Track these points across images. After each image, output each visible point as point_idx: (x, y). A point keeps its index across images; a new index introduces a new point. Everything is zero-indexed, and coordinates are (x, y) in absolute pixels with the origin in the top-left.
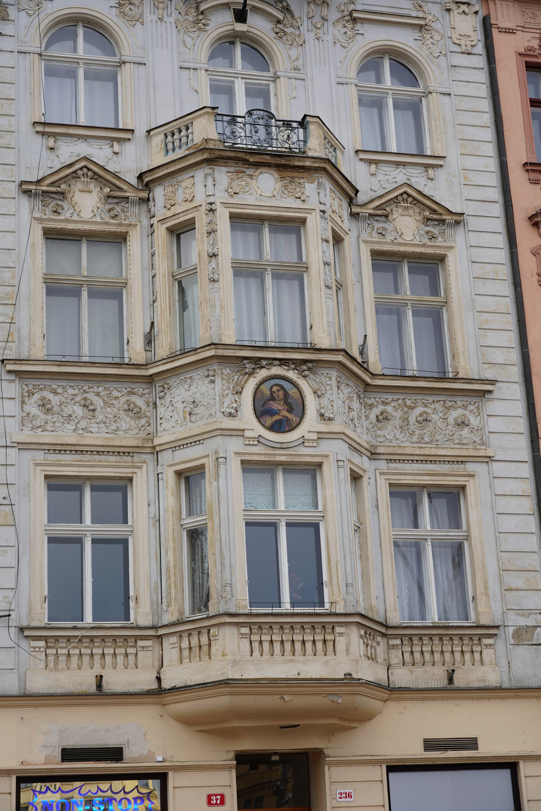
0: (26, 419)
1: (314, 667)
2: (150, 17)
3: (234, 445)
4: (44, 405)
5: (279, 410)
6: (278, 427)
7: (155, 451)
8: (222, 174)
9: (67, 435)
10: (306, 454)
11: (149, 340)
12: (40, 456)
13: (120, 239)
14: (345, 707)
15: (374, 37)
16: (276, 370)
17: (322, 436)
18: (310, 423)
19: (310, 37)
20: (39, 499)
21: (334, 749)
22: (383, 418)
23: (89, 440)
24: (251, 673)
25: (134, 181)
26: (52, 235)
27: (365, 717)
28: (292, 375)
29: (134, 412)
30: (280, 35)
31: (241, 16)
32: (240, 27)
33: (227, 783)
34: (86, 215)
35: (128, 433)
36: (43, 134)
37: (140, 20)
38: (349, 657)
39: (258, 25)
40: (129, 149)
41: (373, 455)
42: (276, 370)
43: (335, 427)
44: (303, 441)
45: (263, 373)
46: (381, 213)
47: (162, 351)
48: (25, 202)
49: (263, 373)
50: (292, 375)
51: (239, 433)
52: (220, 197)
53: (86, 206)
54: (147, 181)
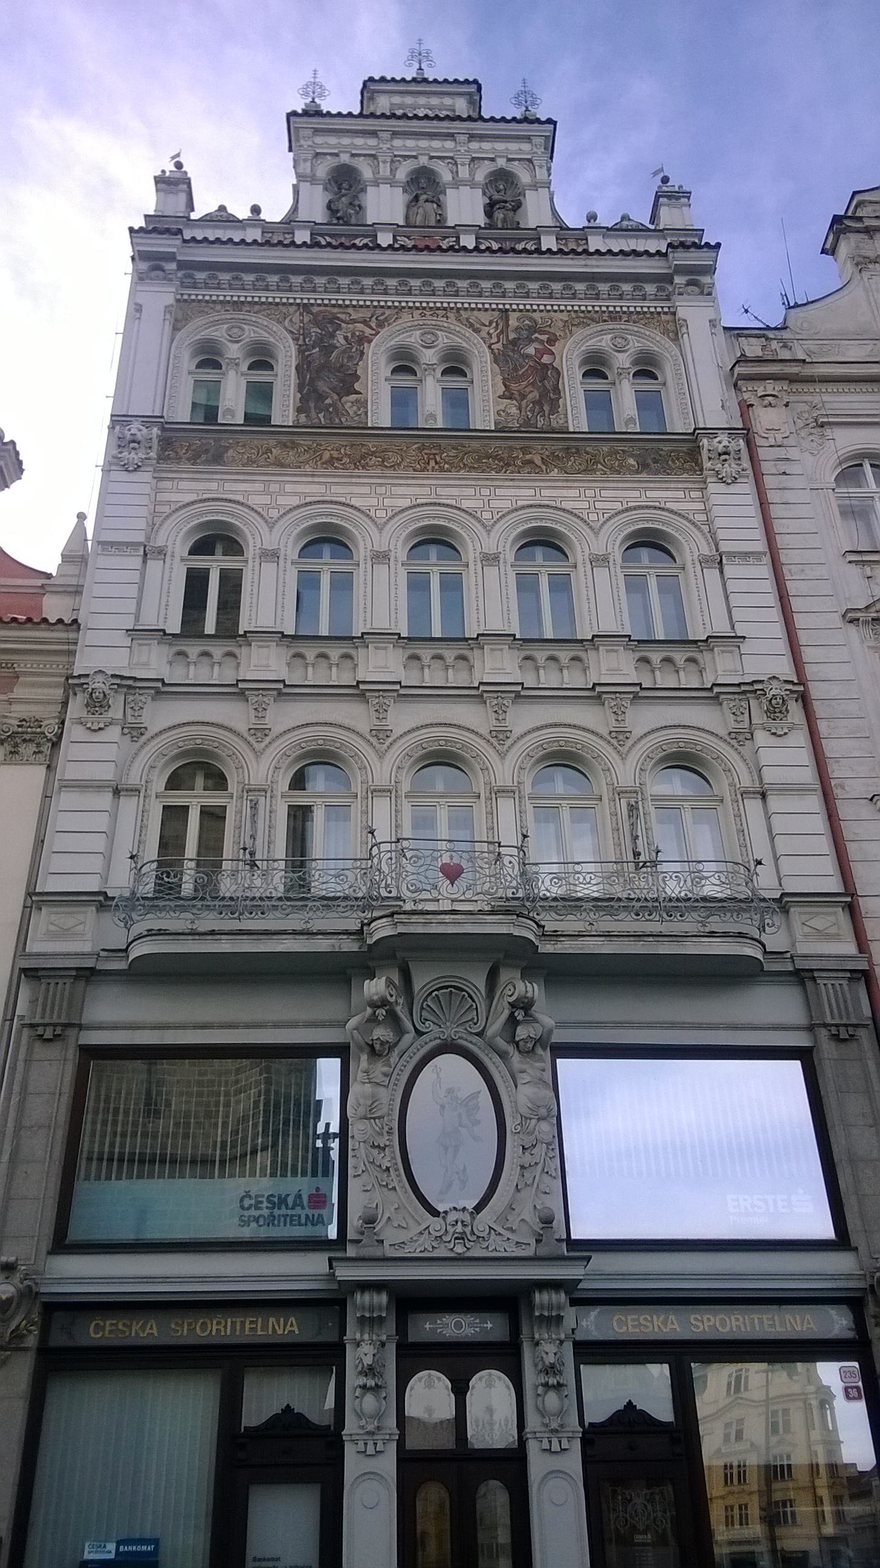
36: (857, 562)
48: (852, 630)
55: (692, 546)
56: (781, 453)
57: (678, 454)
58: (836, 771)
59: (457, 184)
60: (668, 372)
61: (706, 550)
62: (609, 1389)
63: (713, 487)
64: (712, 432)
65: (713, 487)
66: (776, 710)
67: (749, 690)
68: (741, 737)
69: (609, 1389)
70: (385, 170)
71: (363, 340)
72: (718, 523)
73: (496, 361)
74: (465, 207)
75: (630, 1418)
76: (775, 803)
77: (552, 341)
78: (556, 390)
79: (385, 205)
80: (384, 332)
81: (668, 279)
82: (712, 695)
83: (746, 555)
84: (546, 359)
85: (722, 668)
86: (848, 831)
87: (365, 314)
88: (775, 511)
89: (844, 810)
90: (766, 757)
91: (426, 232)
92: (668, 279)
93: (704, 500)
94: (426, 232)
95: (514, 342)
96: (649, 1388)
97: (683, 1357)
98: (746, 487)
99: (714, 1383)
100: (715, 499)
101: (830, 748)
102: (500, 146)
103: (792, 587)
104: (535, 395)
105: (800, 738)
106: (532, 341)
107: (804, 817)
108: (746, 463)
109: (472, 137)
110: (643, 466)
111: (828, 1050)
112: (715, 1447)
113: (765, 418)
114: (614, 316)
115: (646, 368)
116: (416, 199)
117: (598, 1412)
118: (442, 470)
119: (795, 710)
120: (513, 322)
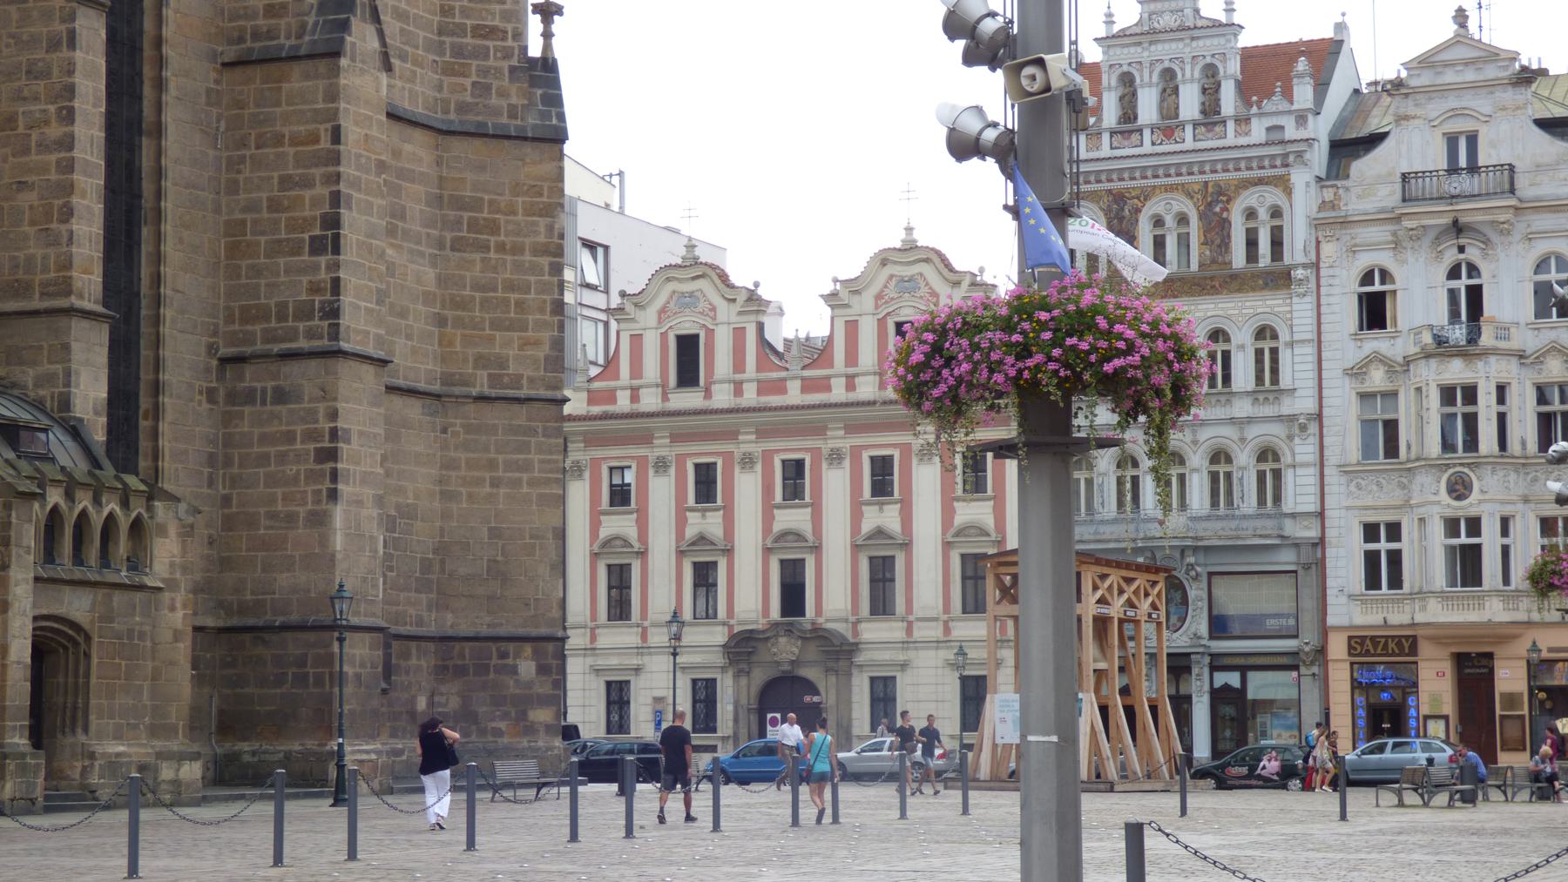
0: (1350, 494)
1: (1473, 616)
2: (1411, 260)
3: (1436, 509)
4: (1359, 487)
5: (1459, 489)
6: (1459, 498)
7: (1411, 507)
8: (1433, 362)
9: (1369, 502)
10: (1473, 512)
11: (1409, 447)
12: (1356, 512)
13: (1395, 394)
14: (1505, 634)
15: (1542, 247)
16: (1458, 469)
17: (1480, 502)
18: (1475, 495)
19: (1502, 256)
20: (1359, 533)
21: (1499, 652)
22: (1535, 480)
23: (1380, 503)
24: (1442, 619)
25: (1400, 360)
26: (1364, 396)
27: (1515, 637)
28: (1466, 470)
29: (1403, 487)
30: (1485, 256)
31: (1461, 249)
32: (1462, 256)
33: (1447, 667)
34: (1377, 382)
35: (1397, 497)
37: (1404, 262)
38: (1495, 611)
39: (1473, 254)
40: (1399, 341)
41: (1526, 500)
42: (1458, 469)
43: (1487, 497)
44: (1471, 505)
45: (1451, 471)
46: (1539, 359)
47: (1413, 456)
48: (1347, 380)
49: (1451, 471)
50: (1466, 470)
51: (1438, 503)
52: (1432, 376)
53: (1377, 379)
54: (1407, 362)
55: (1284, 336)
56: (1331, 272)
57: (1280, 279)
58: (1326, 453)
59: (1184, 82)
60: (1286, 215)
61: (1288, 339)
62: (1221, 679)
63: (1295, 300)
64: (1296, 267)
65: (1295, 300)
66: (1303, 428)
67: (1291, 418)
68: (1290, 438)
69: (1221, 679)
70: (1146, 78)
71: (1138, 211)
72: (1295, 322)
73: (1200, 218)
74: (1190, 103)
75: (1226, 687)
76: (1299, 471)
77: (1228, 201)
78: (1229, 236)
79: (1148, 109)
80: (1148, 204)
81: (1286, 155)
82: (1280, 418)
83: (1303, 341)
84: (1225, 215)
85: (1287, 407)
86: (1327, 480)
87: (1138, 192)
88: (1323, 309)
89: (1327, 471)
90: (1298, 449)
91: (1169, 126)
92: (1286, 155)
93: (1291, 305)
94: (1169, 126)
95: (1210, 204)
96: (1233, 679)
97: (1243, 670)
98: (1310, 299)
99: (1255, 678)
100: (1295, 307)
101: (1327, 441)
102: (1208, 42)
103: (1324, 355)
104: (1218, 241)
105: (1313, 440)
106: (1218, 201)
107: (1308, 477)
108: (1313, 285)
109: (1193, 39)
110: (1266, 286)
111: (1301, 572)
112: (1250, 696)
113: (1328, 249)
114: (1260, 181)
115: (1276, 213)
116: (1164, 90)
117: (1217, 685)
118: (1175, 297)
119: (1313, 428)
120: (1210, 190)
